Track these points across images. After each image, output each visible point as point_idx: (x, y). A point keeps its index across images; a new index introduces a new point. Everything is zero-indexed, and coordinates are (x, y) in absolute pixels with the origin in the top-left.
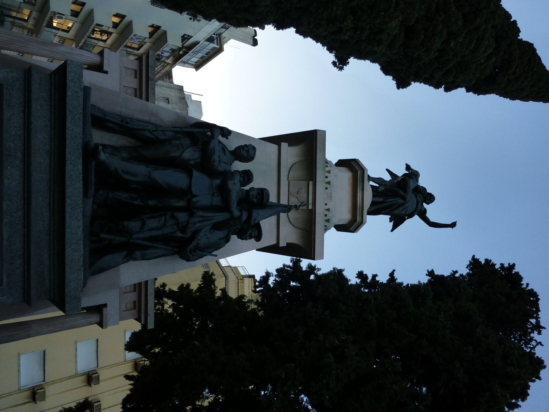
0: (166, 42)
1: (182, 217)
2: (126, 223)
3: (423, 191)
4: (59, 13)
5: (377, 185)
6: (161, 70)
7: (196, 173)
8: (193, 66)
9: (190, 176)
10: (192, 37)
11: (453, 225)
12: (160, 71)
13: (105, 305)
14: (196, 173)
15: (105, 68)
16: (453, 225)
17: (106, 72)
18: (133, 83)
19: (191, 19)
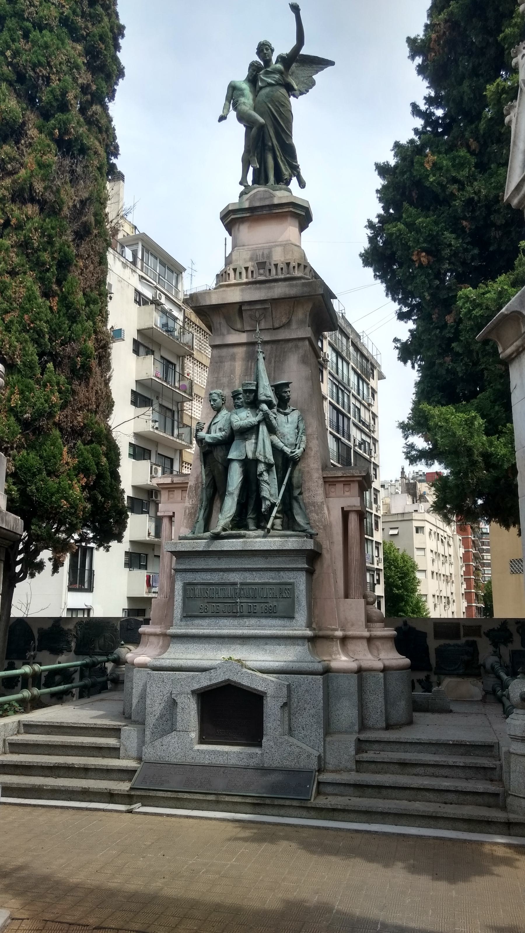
0: (152, 328)
1: (261, 467)
2: (263, 510)
3: (254, 71)
4: (151, 473)
5: (251, 169)
6: (196, 325)
7: (230, 457)
8: (180, 278)
9: (231, 460)
10: (136, 290)
11: (295, 8)
12: (198, 327)
13: (342, 508)
14: (230, 457)
15: (171, 514)
16: (295, 8)
17: (174, 513)
18: (178, 494)
19: (111, 298)
